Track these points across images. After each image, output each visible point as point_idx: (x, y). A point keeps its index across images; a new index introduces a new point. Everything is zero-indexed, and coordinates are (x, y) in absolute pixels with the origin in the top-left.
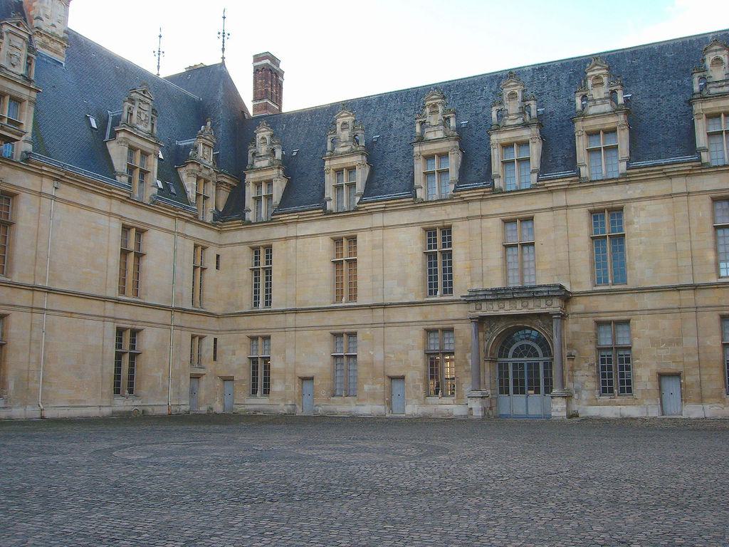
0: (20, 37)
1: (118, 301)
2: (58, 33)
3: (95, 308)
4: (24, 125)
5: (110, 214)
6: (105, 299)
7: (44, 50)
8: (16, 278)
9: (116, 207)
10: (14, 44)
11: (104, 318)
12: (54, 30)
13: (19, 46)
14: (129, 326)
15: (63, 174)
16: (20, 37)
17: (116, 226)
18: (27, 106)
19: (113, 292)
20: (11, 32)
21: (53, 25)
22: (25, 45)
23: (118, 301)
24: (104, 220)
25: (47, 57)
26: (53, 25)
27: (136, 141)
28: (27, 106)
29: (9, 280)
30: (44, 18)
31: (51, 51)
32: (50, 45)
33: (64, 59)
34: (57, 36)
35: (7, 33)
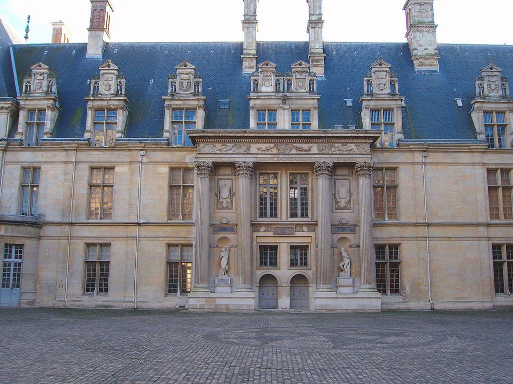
0: (383, 71)
1: (489, 225)
3: (470, 232)
5: (473, 164)
6: (478, 225)
7: (422, 67)
8: (403, 220)
9: (477, 158)
10: (380, 77)
11: (479, 238)
12: (426, 52)
13: (383, 77)
14: (504, 242)
15: (427, 147)
17: (481, 172)
19: (485, 218)
20: (376, 71)
23: (489, 225)
24: (468, 170)
25: (425, 71)
27: (488, 107)
29: (399, 222)
30: (418, 48)
31: (427, 66)
32: (426, 62)
34: (431, 55)
35: (374, 73)
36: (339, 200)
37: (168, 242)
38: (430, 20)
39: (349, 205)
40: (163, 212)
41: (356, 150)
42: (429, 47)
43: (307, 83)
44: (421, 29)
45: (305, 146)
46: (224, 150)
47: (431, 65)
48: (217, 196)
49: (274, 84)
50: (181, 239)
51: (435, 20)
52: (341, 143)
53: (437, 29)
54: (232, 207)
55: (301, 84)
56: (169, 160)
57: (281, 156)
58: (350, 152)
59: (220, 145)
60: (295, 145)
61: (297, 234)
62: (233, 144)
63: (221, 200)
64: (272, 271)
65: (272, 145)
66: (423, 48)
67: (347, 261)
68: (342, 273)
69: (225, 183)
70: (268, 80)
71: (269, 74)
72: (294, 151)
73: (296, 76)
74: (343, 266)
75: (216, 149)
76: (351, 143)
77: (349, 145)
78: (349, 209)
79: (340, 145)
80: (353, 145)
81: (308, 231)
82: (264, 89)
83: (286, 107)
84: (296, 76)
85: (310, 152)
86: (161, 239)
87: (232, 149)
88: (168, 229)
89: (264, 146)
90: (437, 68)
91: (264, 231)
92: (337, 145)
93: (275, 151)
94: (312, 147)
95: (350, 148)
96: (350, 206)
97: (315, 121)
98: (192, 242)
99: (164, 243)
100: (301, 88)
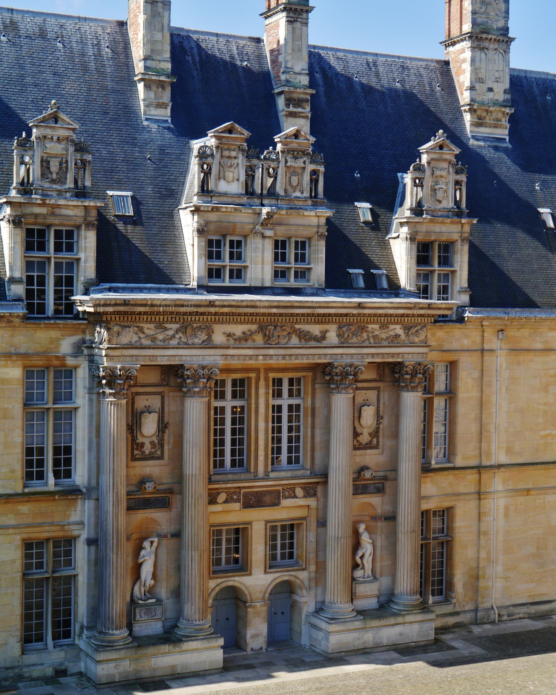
2: (496, 97)
4: (458, 272)
13: (444, 173)
16: (445, 160)
18: (459, 247)
21: (490, 90)
22: (451, 169)
26: (490, 90)
28: (459, 247)
29: (451, 465)
31: (490, 127)
33: (507, 132)
36: (359, 430)
37: (25, 536)
38: (501, 24)
39: (375, 440)
40: (13, 471)
41: (403, 337)
42: (494, 86)
43: (306, 178)
44: (486, 44)
45: (315, 329)
46: (161, 337)
47: (496, 127)
48: (133, 433)
49: (243, 178)
50: (55, 528)
51: (511, 24)
52: (377, 323)
53: (513, 45)
54: (162, 452)
55: (295, 180)
56: (22, 351)
57: (271, 352)
58: (394, 340)
59: (152, 326)
60: (297, 326)
61: (285, 502)
62: (177, 326)
63: (140, 440)
64: (237, 579)
65: (254, 327)
66: (485, 87)
67: (367, 547)
68: (358, 573)
69: (147, 403)
70: (231, 166)
71: (233, 154)
72: (295, 340)
73: (286, 162)
74: (362, 557)
75: (142, 336)
76: (397, 323)
77: (392, 327)
78: (376, 447)
79: (376, 327)
80: (398, 327)
81: (305, 497)
82: (223, 186)
83: (269, 233)
84: (286, 162)
85: (324, 344)
86: (11, 531)
87: (177, 336)
88: (25, 508)
89: (238, 329)
90: (503, 133)
91: (226, 502)
92: (370, 326)
93: (259, 339)
94: (327, 331)
95: (392, 333)
96: (378, 441)
97: (320, 264)
98: (75, 533)
99: (17, 539)
100: (294, 189)
